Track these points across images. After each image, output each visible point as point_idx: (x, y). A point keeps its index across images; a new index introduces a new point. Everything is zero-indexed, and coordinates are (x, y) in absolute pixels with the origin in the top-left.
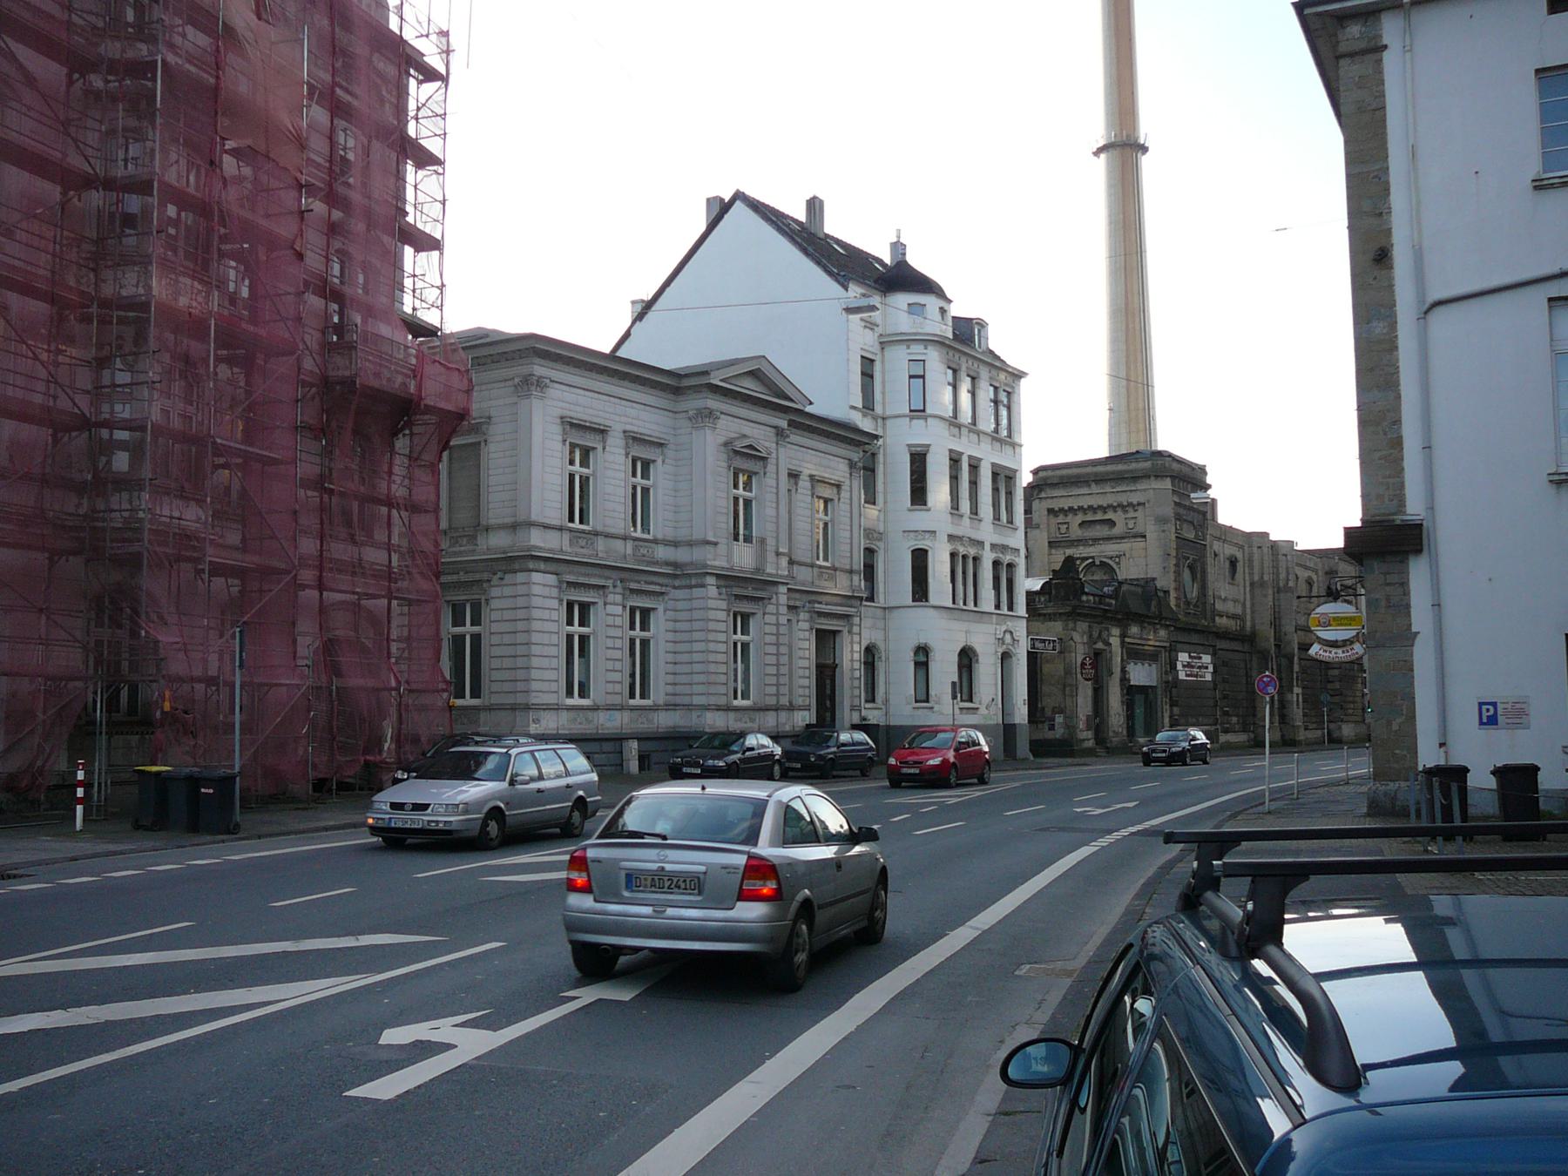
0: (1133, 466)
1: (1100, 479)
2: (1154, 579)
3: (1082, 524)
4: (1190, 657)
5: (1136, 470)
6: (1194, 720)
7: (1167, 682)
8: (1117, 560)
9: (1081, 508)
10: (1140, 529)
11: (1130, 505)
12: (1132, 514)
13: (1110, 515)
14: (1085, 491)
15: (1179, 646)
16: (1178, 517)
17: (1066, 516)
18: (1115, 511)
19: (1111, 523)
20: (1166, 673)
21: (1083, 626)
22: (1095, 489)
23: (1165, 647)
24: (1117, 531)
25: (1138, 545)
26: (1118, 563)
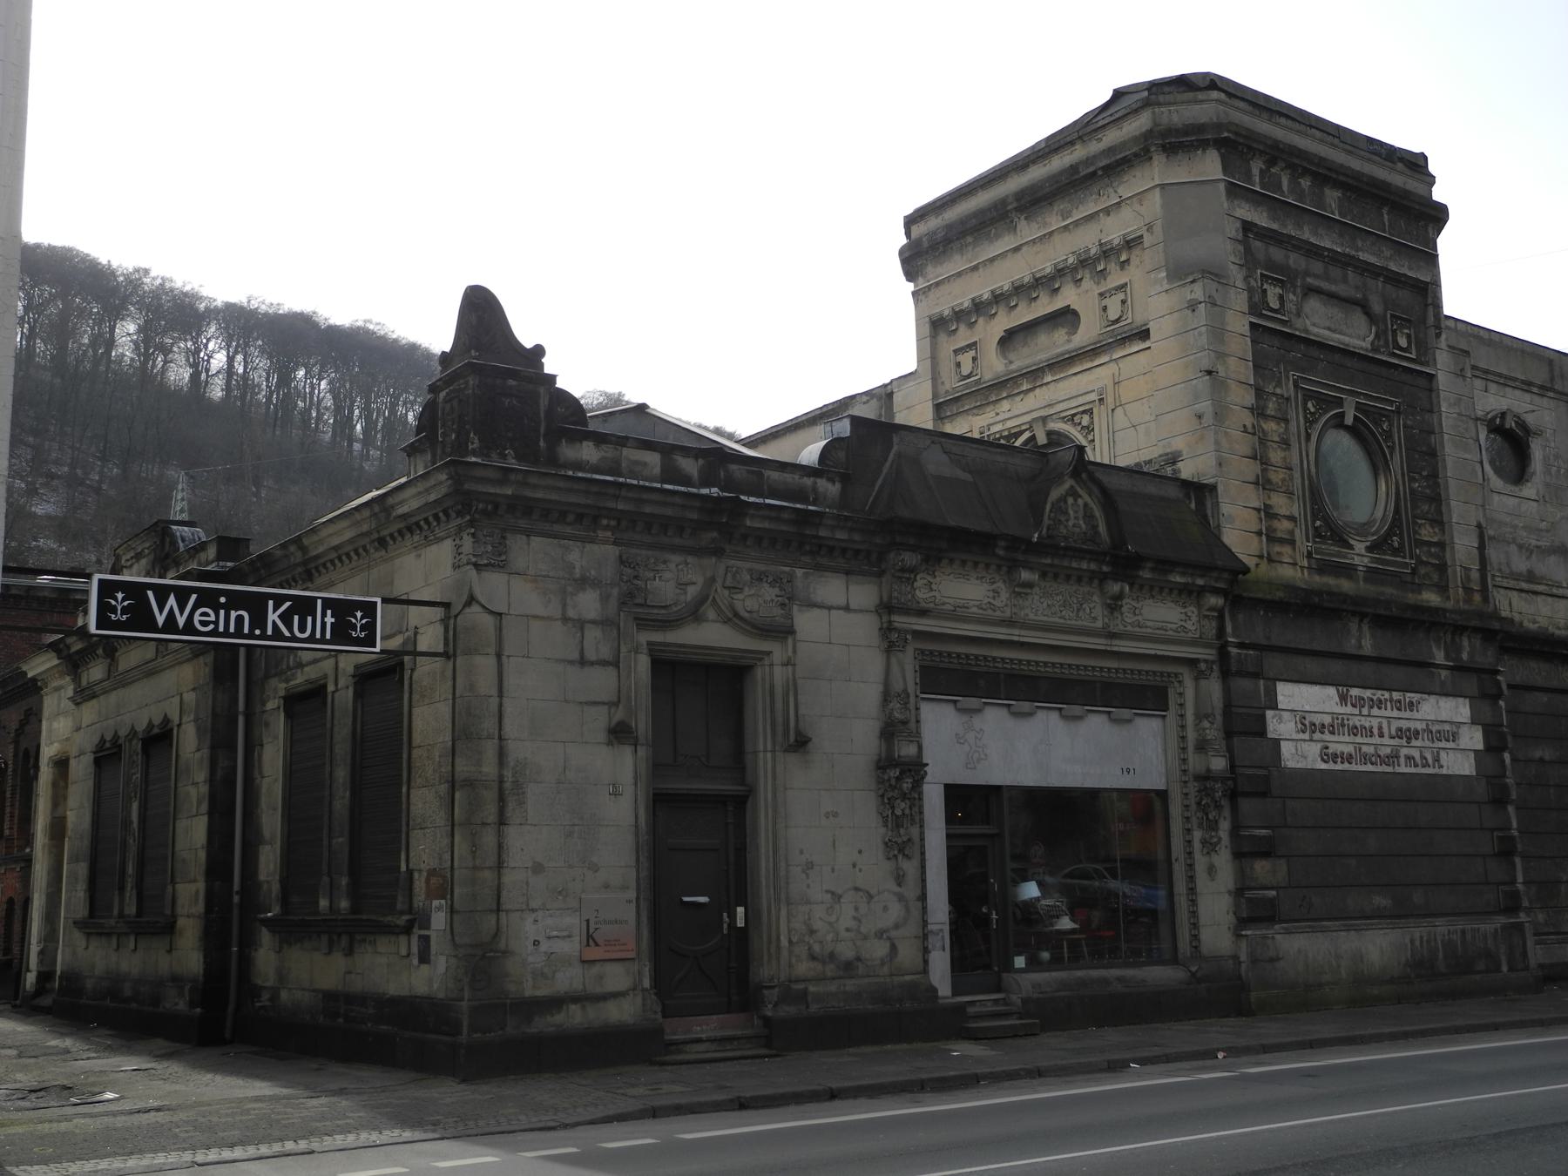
0: (1111, 137)
1: (1033, 202)
2: (1173, 459)
3: (1008, 339)
4: (1343, 699)
5: (1123, 145)
6: (1381, 901)
7: (1205, 777)
8: (1085, 420)
9: (998, 298)
10: (1137, 317)
11: (1107, 252)
12: (1115, 279)
13: (1069, 296)
14: (1005, 243)
15: (1274, 663)
16: (1249, 261)
17: (971, 325)
18: (1078, 282)
19: (1066, 317)
20: (1202, 746)
21: (532, 552)
22: (1027, 230)
23: (1192, 663)
24: (1088, 331)
25: (1132, 364)
26: (1089, 429)
